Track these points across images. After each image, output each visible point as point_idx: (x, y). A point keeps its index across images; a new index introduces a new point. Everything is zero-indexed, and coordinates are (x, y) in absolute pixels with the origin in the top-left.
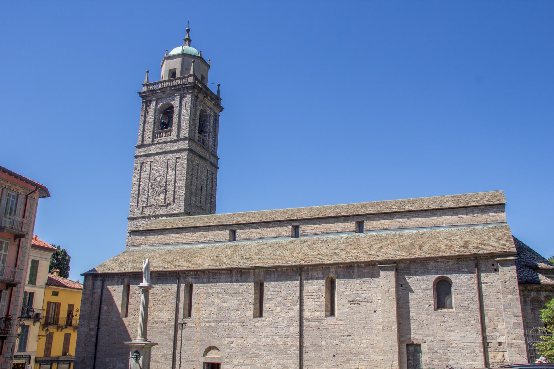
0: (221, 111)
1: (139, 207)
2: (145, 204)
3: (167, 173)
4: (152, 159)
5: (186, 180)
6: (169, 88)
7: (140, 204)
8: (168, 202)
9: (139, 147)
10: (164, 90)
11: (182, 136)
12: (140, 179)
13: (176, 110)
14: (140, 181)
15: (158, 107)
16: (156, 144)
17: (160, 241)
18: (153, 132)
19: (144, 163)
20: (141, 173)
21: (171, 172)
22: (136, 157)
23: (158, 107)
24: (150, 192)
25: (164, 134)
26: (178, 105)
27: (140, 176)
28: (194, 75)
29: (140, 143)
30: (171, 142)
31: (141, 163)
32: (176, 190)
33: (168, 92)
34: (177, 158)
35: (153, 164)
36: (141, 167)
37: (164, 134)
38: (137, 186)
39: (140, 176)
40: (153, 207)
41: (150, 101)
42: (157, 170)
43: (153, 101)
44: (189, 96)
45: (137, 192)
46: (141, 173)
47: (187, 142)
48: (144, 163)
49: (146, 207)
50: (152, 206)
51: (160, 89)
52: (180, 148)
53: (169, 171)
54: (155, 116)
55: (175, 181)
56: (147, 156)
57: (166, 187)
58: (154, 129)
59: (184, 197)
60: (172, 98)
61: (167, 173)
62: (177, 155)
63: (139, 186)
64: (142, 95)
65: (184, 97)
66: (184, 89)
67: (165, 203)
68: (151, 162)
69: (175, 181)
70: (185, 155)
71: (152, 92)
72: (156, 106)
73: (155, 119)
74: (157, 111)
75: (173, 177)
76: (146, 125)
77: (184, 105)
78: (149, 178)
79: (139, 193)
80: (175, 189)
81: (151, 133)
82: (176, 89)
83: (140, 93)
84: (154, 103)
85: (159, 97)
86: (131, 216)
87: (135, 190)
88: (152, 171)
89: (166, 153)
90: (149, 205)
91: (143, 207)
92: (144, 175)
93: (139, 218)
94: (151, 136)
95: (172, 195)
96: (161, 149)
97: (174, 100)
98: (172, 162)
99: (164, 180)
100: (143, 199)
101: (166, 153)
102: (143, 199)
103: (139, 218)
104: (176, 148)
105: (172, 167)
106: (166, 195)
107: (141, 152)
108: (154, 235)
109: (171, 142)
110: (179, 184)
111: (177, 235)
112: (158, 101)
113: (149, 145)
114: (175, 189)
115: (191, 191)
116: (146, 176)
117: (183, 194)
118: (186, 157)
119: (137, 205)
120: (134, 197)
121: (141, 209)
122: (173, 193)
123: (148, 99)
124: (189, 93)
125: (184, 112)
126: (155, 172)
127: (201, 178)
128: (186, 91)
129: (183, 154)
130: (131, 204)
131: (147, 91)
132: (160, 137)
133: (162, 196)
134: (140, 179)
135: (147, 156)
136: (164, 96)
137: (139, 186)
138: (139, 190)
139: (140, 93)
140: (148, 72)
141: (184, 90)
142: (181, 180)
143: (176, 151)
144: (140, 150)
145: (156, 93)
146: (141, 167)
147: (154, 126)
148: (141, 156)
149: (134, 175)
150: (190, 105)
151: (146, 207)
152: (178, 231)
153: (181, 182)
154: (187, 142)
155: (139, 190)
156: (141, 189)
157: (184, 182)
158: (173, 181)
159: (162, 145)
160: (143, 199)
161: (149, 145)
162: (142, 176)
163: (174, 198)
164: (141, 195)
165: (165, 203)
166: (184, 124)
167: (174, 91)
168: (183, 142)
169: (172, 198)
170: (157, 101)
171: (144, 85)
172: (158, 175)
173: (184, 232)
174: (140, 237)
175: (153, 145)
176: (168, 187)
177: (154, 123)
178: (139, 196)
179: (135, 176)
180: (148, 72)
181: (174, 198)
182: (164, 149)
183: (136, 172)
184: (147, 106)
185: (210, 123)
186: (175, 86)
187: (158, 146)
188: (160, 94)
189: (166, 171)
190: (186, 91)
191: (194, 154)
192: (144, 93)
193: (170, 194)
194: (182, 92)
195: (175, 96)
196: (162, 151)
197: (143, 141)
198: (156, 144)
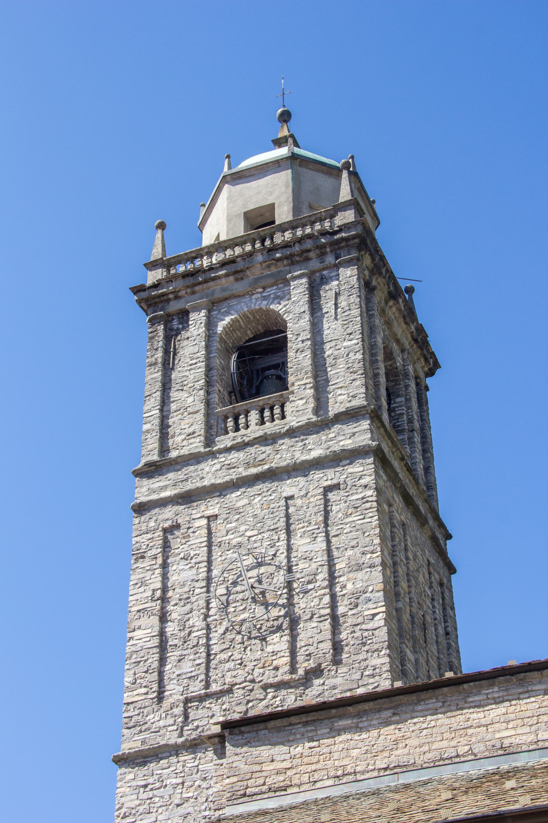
0: (431, 373)
1: (166, 704)
2: (197, 688)
3: (289, 549)
4: (213, 506)
5: (383, 564)
6: (259, 258)
7: (174, 691)
8: (312, 664)
9: (151, 470)
10: (240, 265)
11: (339, 401)
12: (165, 589)
13: (297, 329)
14: (164, 599)
15: (220, 329)
16: (228, 450)
17: (400, 755)
18: (208, 415)
19: (177, 526)
20: (165, 566)
21: (308, 546)
22: (141, 509)
23: (220, 329)
24: (215, 637)
25: (254, 416)
26: (306, 307)
27: (165, 577)
28: (353, 204)
29: (155, 457)
30: (292, 433)
31: (165, 530)
32: (341, 610)
33: (256, 271)
34: (328, 489)
35: (219, 527)
36: (166, 546)
37: (254, 416)
38: (155, 621)
39: (165, 577)
40: (238, 693)
41: (184, 315)
42: (240, 545)
43: (197, 309)
44: (349, 275)
45: (156, 641)
46: (165, 566)
47: (365, 424)
48: (177, 526)
49: (201, 699)
50: (230, 691)
51: (223, 264)
52: (337, 448)
53: (298, 542)
54: (208, 358)
55: (332, 578)
56: (187, 498)
57: (290, 604)
58: (208, 403)
59: (383, 634)
60: (271, 291)
61: (289, 549)
62: (330, 476)
63: (163, 618)
64: (150, 300)
65: (324, 281)
66: (321, 251)
67: (293, 669)
68: (211, 518)
69: (332, 578)
70: (364, 471)
71: (190, 281)
72: (210, 325)
73: (209, 369)
74: (216, 345)
75: (322, 558)
76: (174, 395)
77: (328, 306)
78: (209, 580)
79: (163, 646)
80: (333, 605)
81: (200, 417)
82: (292, 256)
83: (137, 290)
84: (198, 320)
85: (218, 295)
86: (131, 744)
87: (144, 634)
88: (217, 553)
89: (273, 475)
90: (214, 688)
91: (187, 701)
92: (181, 574)
93: (174, 750)
94: (199, 427)
95: (328, 635)
96: (248, 465)
97: (287, 296)
98: (308, 507)
99: (280, 578)
100: (187, 667)
101: (273, 475)
102: (182, 671)
103: (174, 750)
104: (316, 453)
105: (305, 529)
106: (294, 638)
107: (164, 486)
108: (358, 729)
109: (292, 433)
110: (349, 584)
111: (496, 712)
112: (214, 306)
113: (196, 459)
114: (333, 605)
115: (399, 620)
116: (190, 574)
117: (380, 621)
118: (369, 479)
119: (160, 698)
120: (142, 667)
121: (179, 710)
122: (327, 625)
123: (174, 306)
124: (348, 263)
125: (331, 328)
126: (231, 555)
127: (416, 579)
128: (330, 259)
129: (356, 468)
130: (127, 697)
131: (170, 280)
132: (237, 429)
133: (279, 643)
134: (165, 589)
135: (187, 498)
136: (239, 287)
137: (163, 618)
138: (162, 634)
139: (137, 290)
140: (162, 226)
141: (322, 255)
142: (359, 568)
143: (318, 464)
144: (156, 483)
145: (206, 281)
146: (166, 546)
147: (208, 393)
148: (163, 503)
149: (134, 578)
150: (355, 299)
151: (201, 699)
152: (495, 691)
153: (360, 575)
154: (365, 424)
155: (162, 634)
156: (171, 628)
157: (377, 576)
158: (323, 575)
159: (252, 450)
160: (187, 667)
161: (196, 459)
162: (173, 578)
163: (337, 647)
164: (173, 656)
165: (293, 669)
166: (342, 364)
167: (282, 267)
168: (349, 429)
169: (327, 646)
170: (209, 311)
171: (152, 265)
172: (250, 561)
173: (530, 693)
174: (279, 751)
175: (213, 455)
176: (302, 604)
177: (209, 384)
178: (162, 661)
179: (143, 583)
180: (162, 226)
181: (337, 647)
182: (262, 462)
183: (146, 563)
184: (171, 336)
185: (408, 400)
186: (286, 245)
187: (234, 456)
188: (225, 283)
189: (282, 544)
190: (330, 259)
191: (390, 479)
192: (155, 286)
193: (314, 635)
194: (315, 264)
195: (287, 283)
196: (254, 471)
197: (164, 449)
198: (228, 450)
